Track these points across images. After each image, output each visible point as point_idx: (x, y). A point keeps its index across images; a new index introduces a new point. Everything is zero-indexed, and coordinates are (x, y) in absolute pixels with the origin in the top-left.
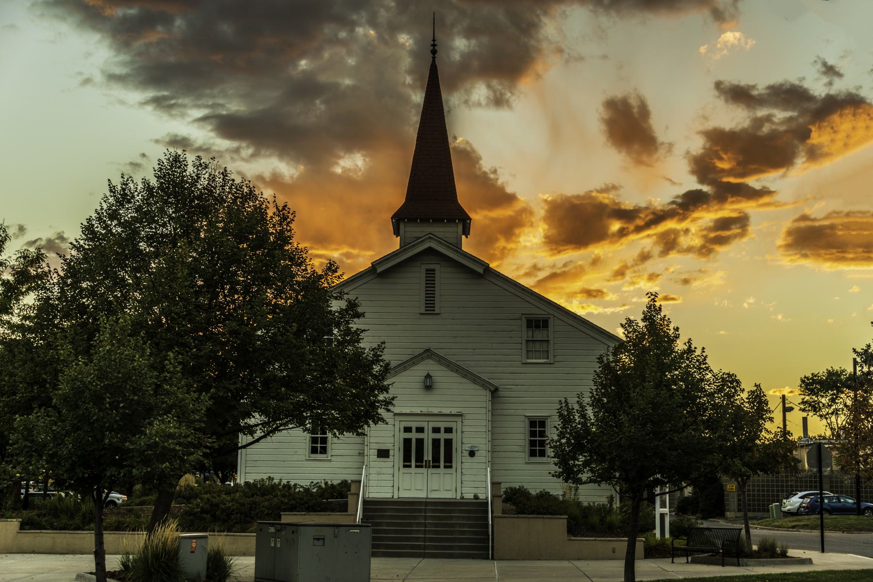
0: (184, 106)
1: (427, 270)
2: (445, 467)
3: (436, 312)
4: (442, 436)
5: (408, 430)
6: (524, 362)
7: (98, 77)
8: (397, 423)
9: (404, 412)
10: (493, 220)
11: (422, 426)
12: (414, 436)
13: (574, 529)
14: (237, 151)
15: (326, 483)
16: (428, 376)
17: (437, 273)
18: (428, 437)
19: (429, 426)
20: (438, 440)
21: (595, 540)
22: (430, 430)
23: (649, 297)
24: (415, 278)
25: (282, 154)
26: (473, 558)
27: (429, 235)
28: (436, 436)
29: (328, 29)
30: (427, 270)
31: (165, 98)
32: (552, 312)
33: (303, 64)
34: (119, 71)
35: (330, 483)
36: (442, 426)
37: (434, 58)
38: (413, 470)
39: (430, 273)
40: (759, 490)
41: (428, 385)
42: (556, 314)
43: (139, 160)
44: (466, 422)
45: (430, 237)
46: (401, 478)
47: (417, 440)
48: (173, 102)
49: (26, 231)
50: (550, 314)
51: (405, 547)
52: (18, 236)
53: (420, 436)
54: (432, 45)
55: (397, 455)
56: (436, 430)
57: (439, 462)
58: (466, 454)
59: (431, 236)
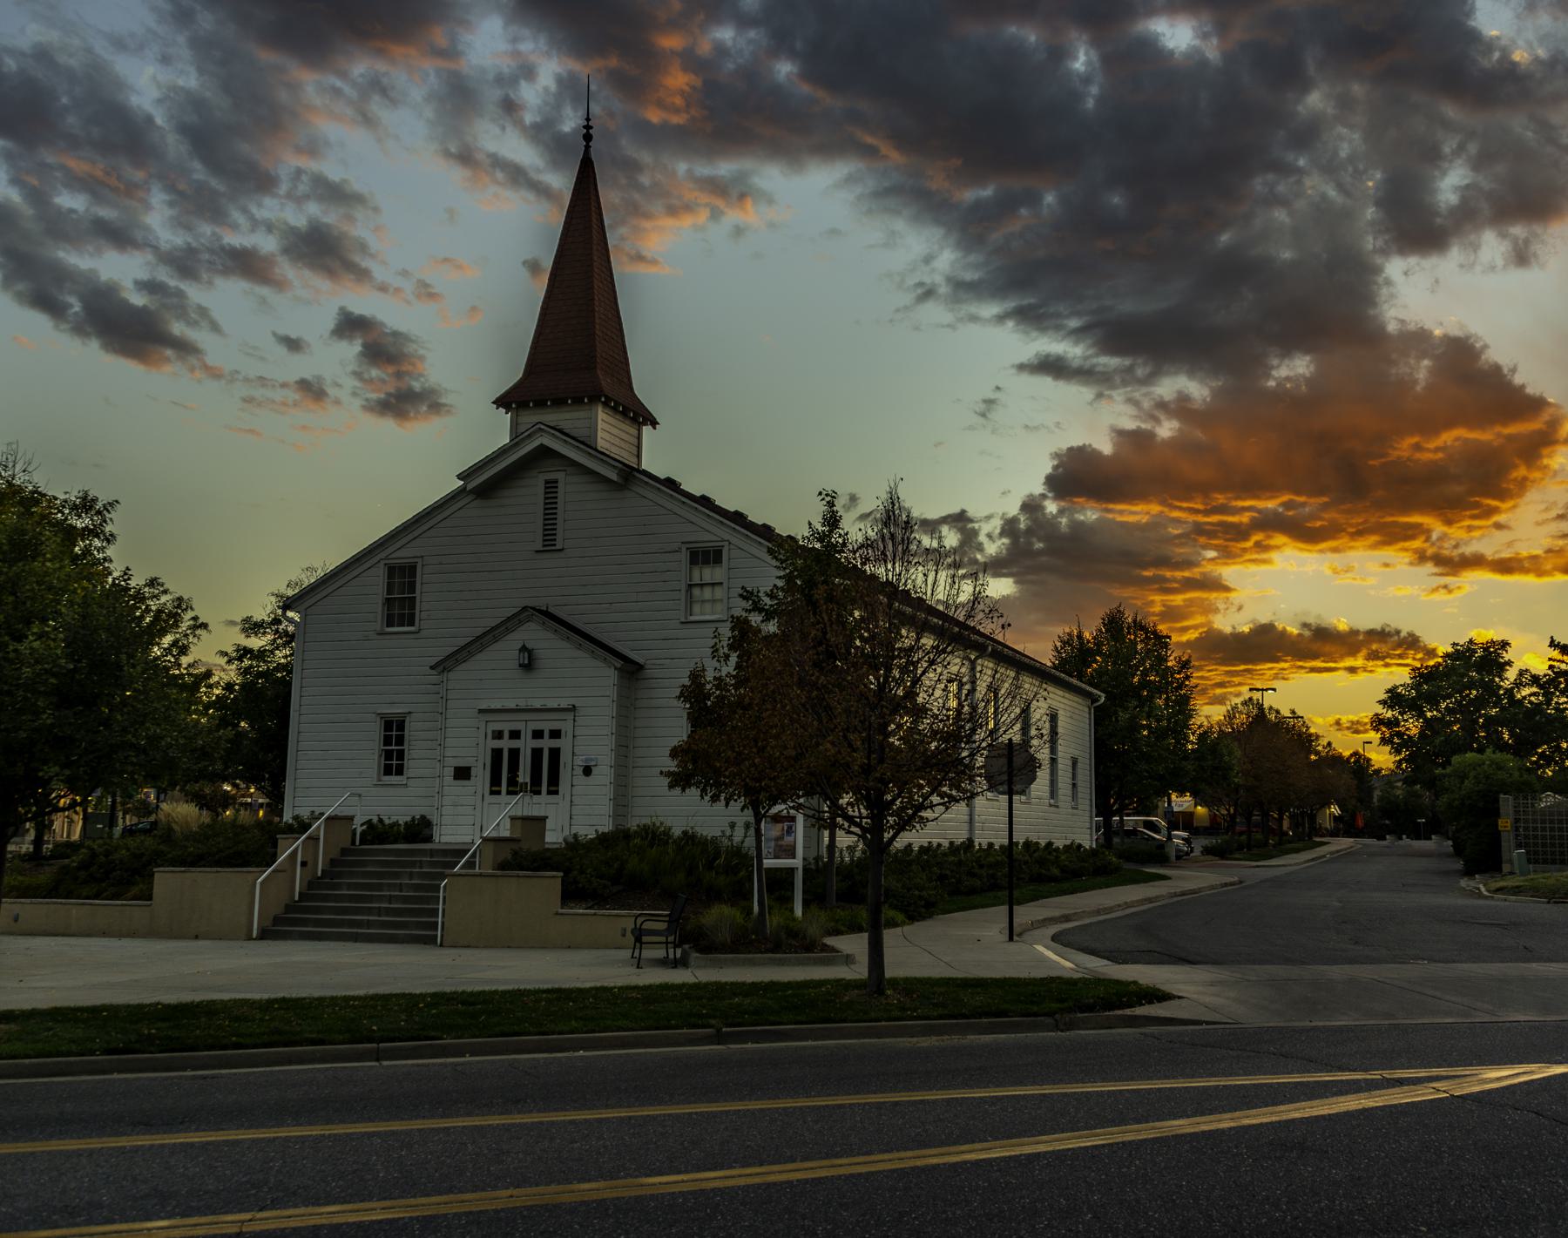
0: (1058, 315)
1: (547, 482)
2: (550, 793)
3: (557, 547)
4: (546, 743)
5: (498, 735)
6: (683, 620)
7: (943, 289)
8: (482, 725)
9: (493, 707)
10: (1510, 438)
11: (517, 729)
12: (506, 744)
13: (570, 895)
14: (1130, 370)
15: (381, 821)
16: (524, 649)
17: (560, 485)
18: (526, 745)
19: (527, 729)
20: (541, 750)
21: (595, 914)
22: (530, 735)
23: (823, 499)
24: (531, 492)
25: (1191, 374)
26: (425, 944)
27: (538, 426)
28: (538, 743)
29: (1259, 184)
30: (547, 482)
31: (1030, 307)
32: (726, 537)
33: (1225, 238)
34: (969, 276)
35: (387, 822)
36: (546, 727)
37: (587, 147)
38: (504, 797)
39: (551, 485)
40: (1552, 829)
41: (529, 662)
42: (734, 540)
43: (992, 396)
44: (580, 721)
45: (540, 429)
46: (485, 810)
47: (551, 750)
48: (1042, 311)
49: (859, 501)
50: (723, 540)
51: (369, 924)
52: (849, 508)
53: (515, 744)
54: (584, 127)
55: (481, 776)
56: (538, 734)
57: (500, 785)
58: (579, 771)
59: (543, 427)
